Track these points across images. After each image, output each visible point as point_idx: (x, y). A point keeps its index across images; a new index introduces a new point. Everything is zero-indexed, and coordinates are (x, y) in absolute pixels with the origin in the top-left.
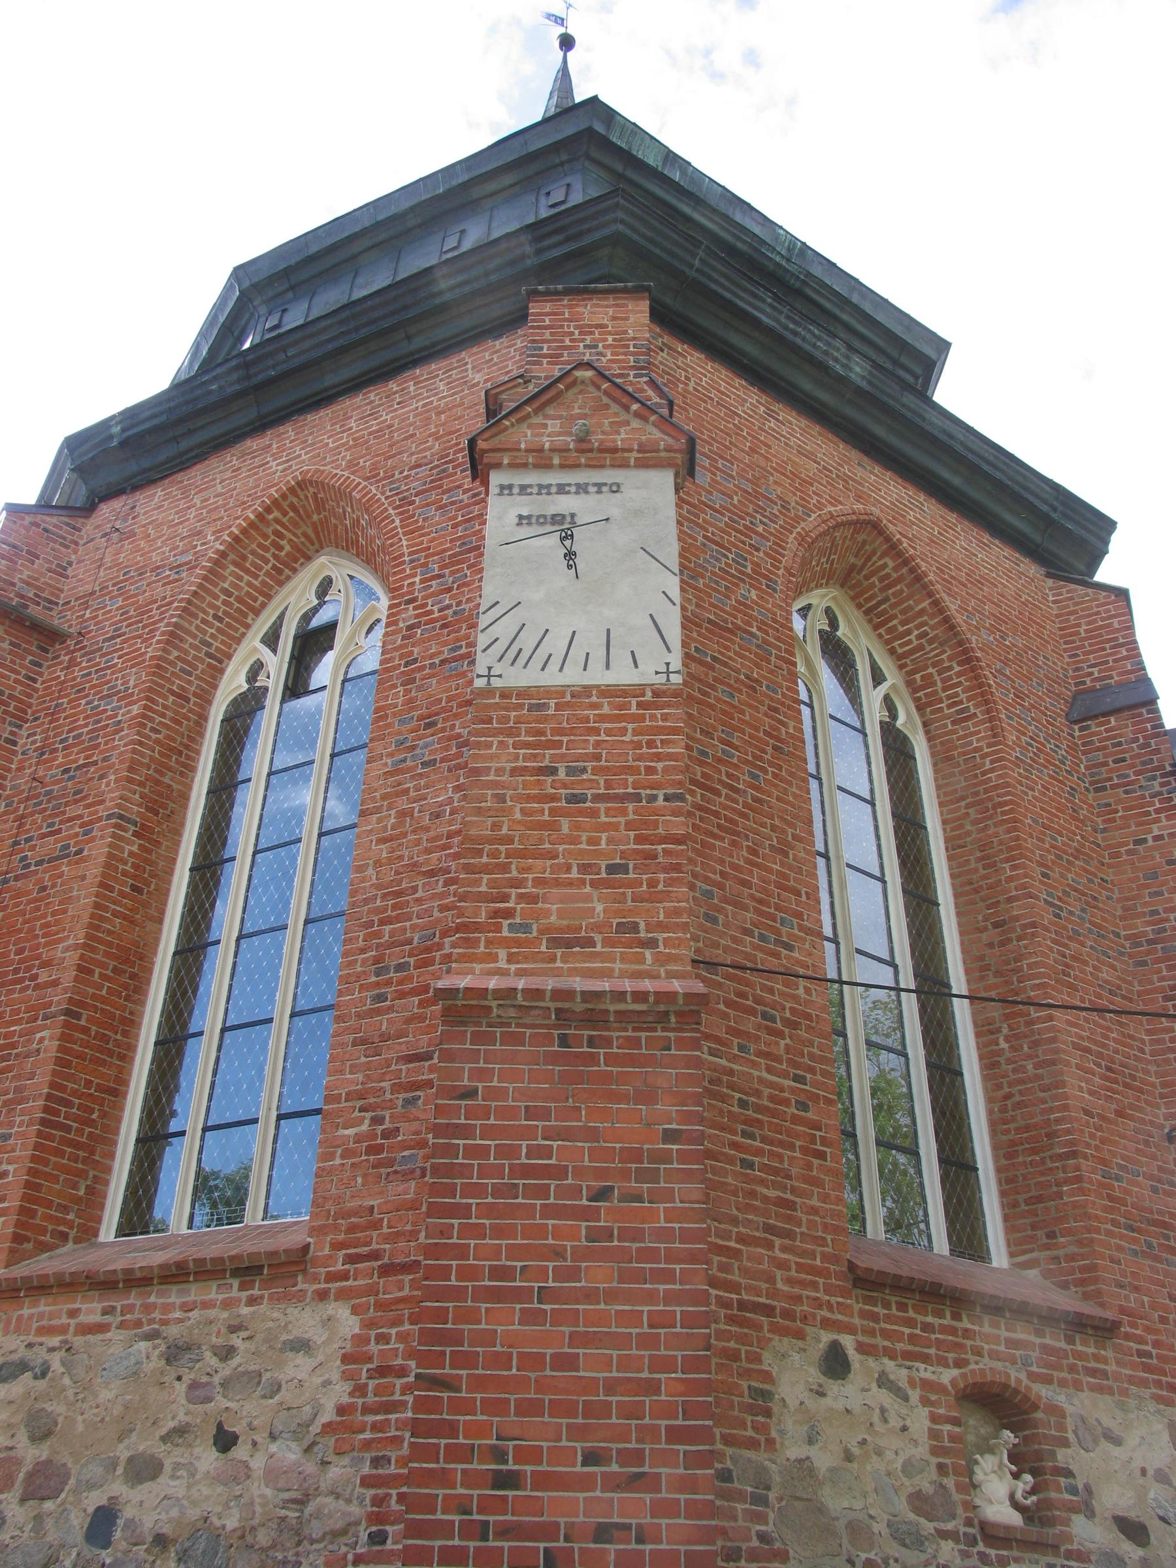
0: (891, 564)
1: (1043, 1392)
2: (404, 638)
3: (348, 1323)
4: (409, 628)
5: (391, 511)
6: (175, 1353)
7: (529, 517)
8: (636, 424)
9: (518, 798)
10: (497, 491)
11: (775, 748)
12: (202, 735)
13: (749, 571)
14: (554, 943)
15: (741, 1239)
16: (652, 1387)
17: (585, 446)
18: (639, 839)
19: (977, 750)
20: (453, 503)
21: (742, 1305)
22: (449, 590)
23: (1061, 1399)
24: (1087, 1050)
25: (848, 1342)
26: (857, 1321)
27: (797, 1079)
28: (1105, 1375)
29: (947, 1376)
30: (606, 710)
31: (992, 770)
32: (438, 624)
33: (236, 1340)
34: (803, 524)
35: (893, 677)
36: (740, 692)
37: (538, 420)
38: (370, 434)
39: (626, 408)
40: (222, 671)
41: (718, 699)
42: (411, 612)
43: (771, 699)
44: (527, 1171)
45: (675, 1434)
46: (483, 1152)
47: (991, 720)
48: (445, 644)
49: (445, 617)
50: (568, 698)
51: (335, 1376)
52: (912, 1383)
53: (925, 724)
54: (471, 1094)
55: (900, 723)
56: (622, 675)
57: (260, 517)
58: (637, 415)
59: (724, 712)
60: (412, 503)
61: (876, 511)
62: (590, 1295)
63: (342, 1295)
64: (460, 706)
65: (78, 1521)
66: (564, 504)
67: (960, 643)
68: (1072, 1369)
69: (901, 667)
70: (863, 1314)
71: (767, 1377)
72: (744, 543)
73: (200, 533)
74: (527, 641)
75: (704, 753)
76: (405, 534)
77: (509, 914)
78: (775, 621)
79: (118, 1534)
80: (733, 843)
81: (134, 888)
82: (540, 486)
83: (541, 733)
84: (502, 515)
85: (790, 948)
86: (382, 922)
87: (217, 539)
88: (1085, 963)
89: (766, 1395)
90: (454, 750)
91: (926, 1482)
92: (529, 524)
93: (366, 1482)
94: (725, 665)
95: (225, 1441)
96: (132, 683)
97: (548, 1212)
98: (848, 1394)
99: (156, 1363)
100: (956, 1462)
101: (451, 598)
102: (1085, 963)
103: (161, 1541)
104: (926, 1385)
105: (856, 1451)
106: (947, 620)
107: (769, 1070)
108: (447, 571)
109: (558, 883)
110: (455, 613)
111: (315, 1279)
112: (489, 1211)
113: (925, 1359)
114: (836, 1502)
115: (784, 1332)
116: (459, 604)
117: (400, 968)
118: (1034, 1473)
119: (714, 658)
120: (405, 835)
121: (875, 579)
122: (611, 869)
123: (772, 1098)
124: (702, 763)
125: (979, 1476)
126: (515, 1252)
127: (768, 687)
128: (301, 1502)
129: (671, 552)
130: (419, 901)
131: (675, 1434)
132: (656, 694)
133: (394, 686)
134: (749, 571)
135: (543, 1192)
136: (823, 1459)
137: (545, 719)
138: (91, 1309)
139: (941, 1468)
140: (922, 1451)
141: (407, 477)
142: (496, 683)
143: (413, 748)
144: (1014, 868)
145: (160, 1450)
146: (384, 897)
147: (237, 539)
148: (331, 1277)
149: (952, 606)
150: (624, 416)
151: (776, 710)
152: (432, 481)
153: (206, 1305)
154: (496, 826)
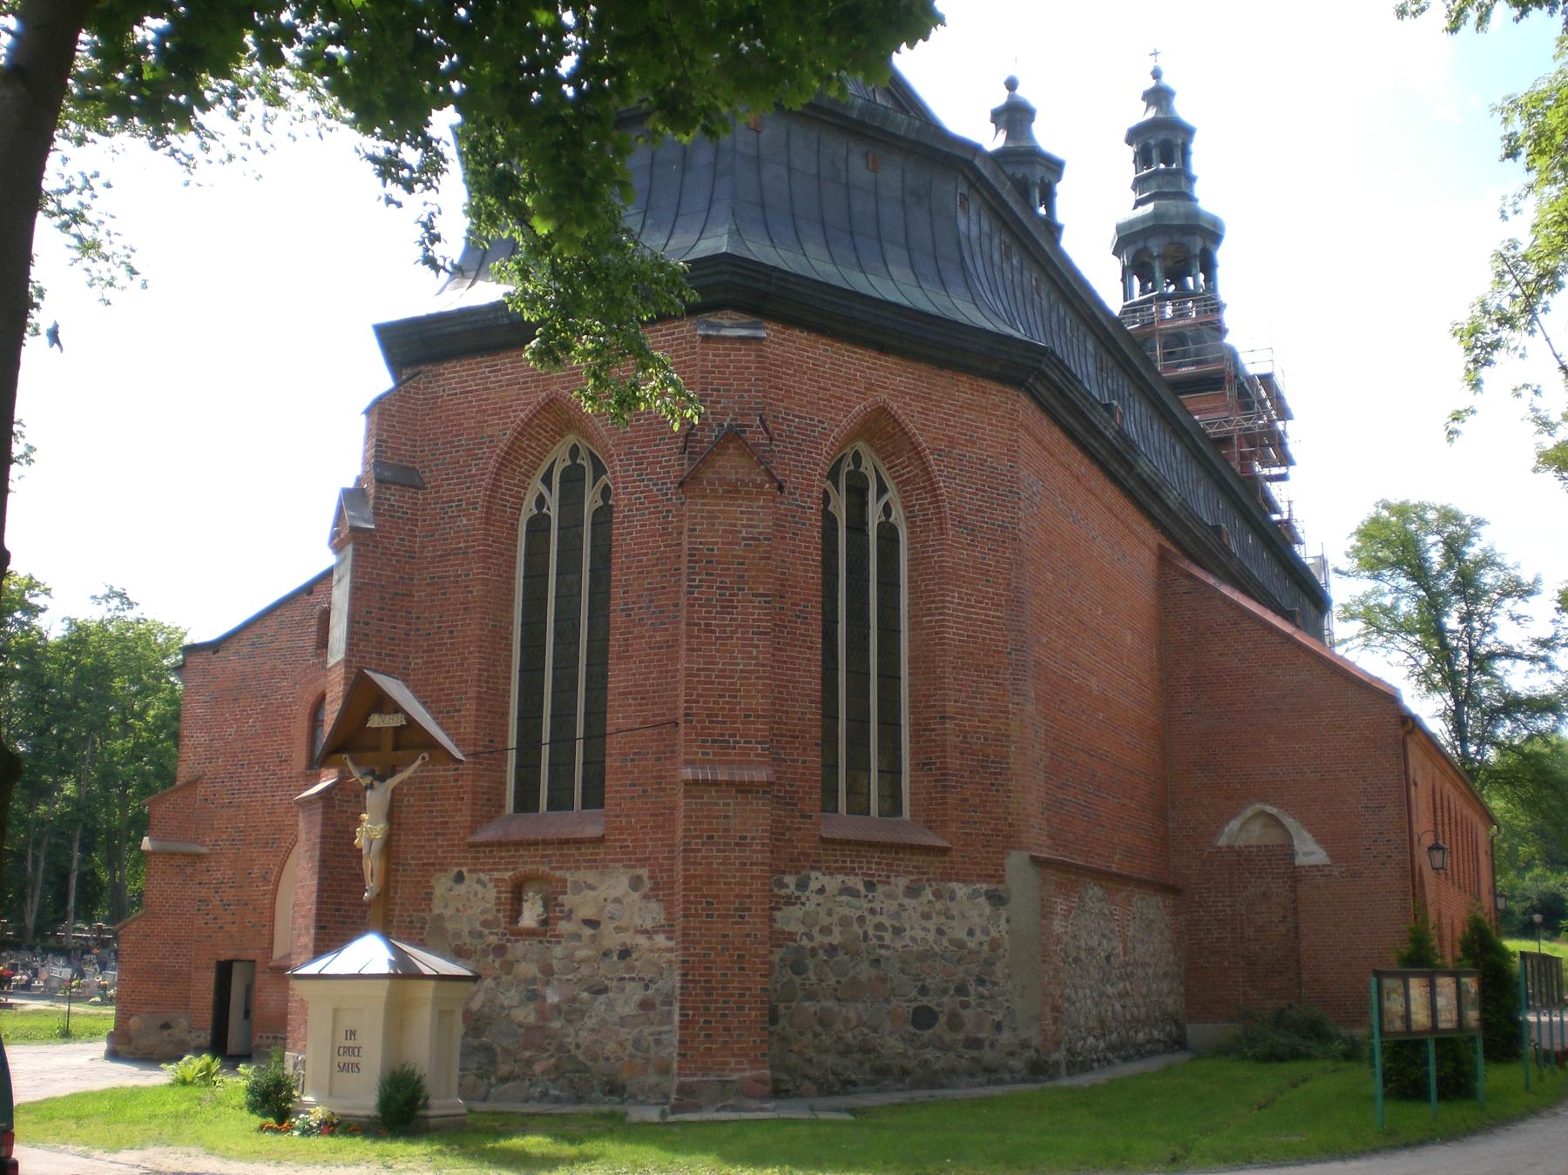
25: (464, 869)
29: (507, 875)
61: (555, 387)
91: (489, 917)
98: (462, 889)
114: (450, 926)
136: (448, 912)
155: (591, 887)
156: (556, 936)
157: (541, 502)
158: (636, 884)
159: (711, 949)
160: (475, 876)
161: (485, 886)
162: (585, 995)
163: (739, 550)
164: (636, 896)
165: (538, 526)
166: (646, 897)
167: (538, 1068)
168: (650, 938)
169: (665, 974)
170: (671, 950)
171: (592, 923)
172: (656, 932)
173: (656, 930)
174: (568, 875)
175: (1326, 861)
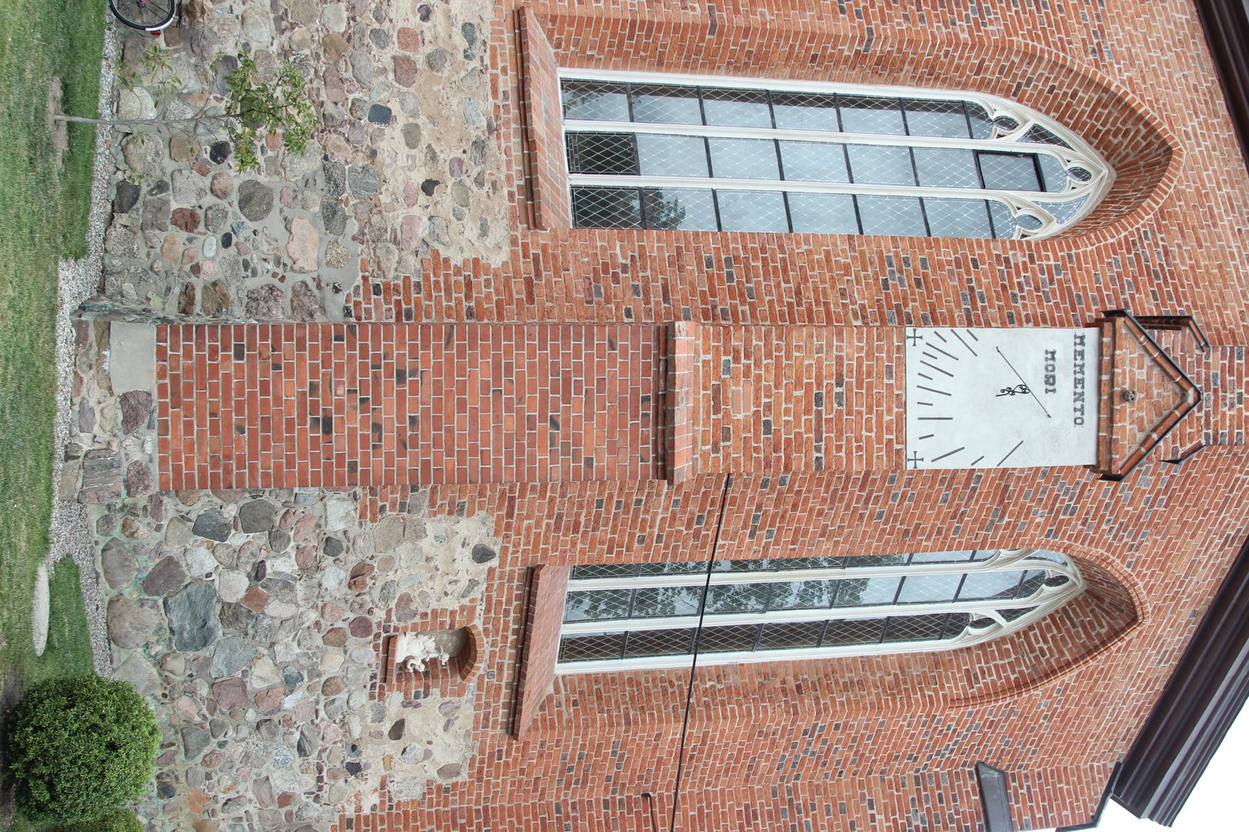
0: (1103, 631)
1: (472, 683)
2: (998, 256)
3: (497, 260)
4: (1007, 260)
5: (1124, 234)
6: (479, 145)
7: (1053, 359)
8: (1140, 436)
9: (819, 361)
10: (1079, 334)
11: (907, 532)
12: (950, 87)
13: (1061, 517)
14: (717, 390)
15: (552, 500)
16: (450, 453)
17: (1116, 399)
18: (788, 441)
19: (942, 686)
20: (1122, 286)
21: (512, 499)
22: (1037, 289)
23: (468, 695)
24: (704, 743)
25: (494, 563)
26: (508, 568)
27: (659, 537)
28: (486, 726)
29: (478, 623)
30: (886, 418)
31: (923, 696)
32: (1006, 283)
33: (488, 186)
34: (1118, 561)
35: (1009, 627)
36: (949, 507)
37: (1147, 361)
38: (1210, 208)
39: (1154, 430)
40: (1007, 96)
41: (939, 491)
42: (1021, 260)
43: (948, 530)
44: (567, 381)
45: (426, 464)
46: (577, 355)
47: (966, 699)
48: (988, 290)
49: (1012, 287)
50: (897, 392)
51: (466, 255)
52: (472, 600)
53: (968, 649)
54: (612, 346)
55: (968, 629)
56: (914, 428)
57: (1141, 118)
58: (1148, 437)
59: (929, 496)
60: (1129, 252)
61: (1148, 622)
62: (498, 418)
63: (514, 254)
64: (931, 304)
65: (380, 97)
66: (1065, 384)
67: (1033, 681)
68: (488, 705)
69: (1018, 634)
70: (512, 572)
71: (471, 513)
72: (1087, 513)
73: (1132, 65)
74: (943, 362)
75: (892, 480)
76: (1098, 249)
77: (737, 359)
78: (1019, 535)
79: (376, 126)
80: (824, 500)
81: (814, 57)
82: (1082, 366)
83: (869, 375)
84: (1061, 339)
85: (752, 535)
86: (764, 259)
87: (1123, 82)
88: (771, 749)
90: (894, 303)
92: (1047, 359)
93: (407, 279)
94: (971, 497)
95: (429, 187)
96: (989, 28)
97: (544, 395)
98: (464, 559)
99: (474, 134)
100: (428, 623)
101: (1029, 291)
102: (771, 749)
103: (374, 153)
104: (472, 610)
105: (432, 564)
106: (1054, 672)
107: (663, 519)
108: (1056, 286)
109: (757, 390)
110: (1014, 296)
111: (524, 236)
112: (543, 361)
113: (488, 610)
114: (403, 551)
115: (498, 523)
116: (1023, 298)
117: (730, 276)
118: (426, 674)
119: (974, 489)
120: (830, 271)
121: (1091, 617)
122: (767, 424)
123: (644, 520)
124: (884, 479)
125: (423, 638)
126: (520, 375)
127: (958, 528)
128: (395, 241)
129: (1018, 462)
130: (778, 285)
131: (426, 464)
132: (898, 451)
133: (955, 252)
134: (1061, 517)
135: (555, 391)
136: (426, 544)
137: (879, 377)
138: (507, 83)
140: (434, 605)
141: (1157, 245)
142: (909, 342)
143: (901, 272)
144: (842, 704)
145: (423, 146)
146: (783, 260)
147: (1120, 100)
148: (525, 246)
149: (1069, 677)
150: (1148, 427)
151: (939, 532)
152: (1148, 267)
153: (509, 163)
154: (799, 348)
156: (381, 695)
162: (297, 735)
164: (432, 773)
166: (430, 783)
167: (184, 703)
170: (359, 809)
171: (398, 730)
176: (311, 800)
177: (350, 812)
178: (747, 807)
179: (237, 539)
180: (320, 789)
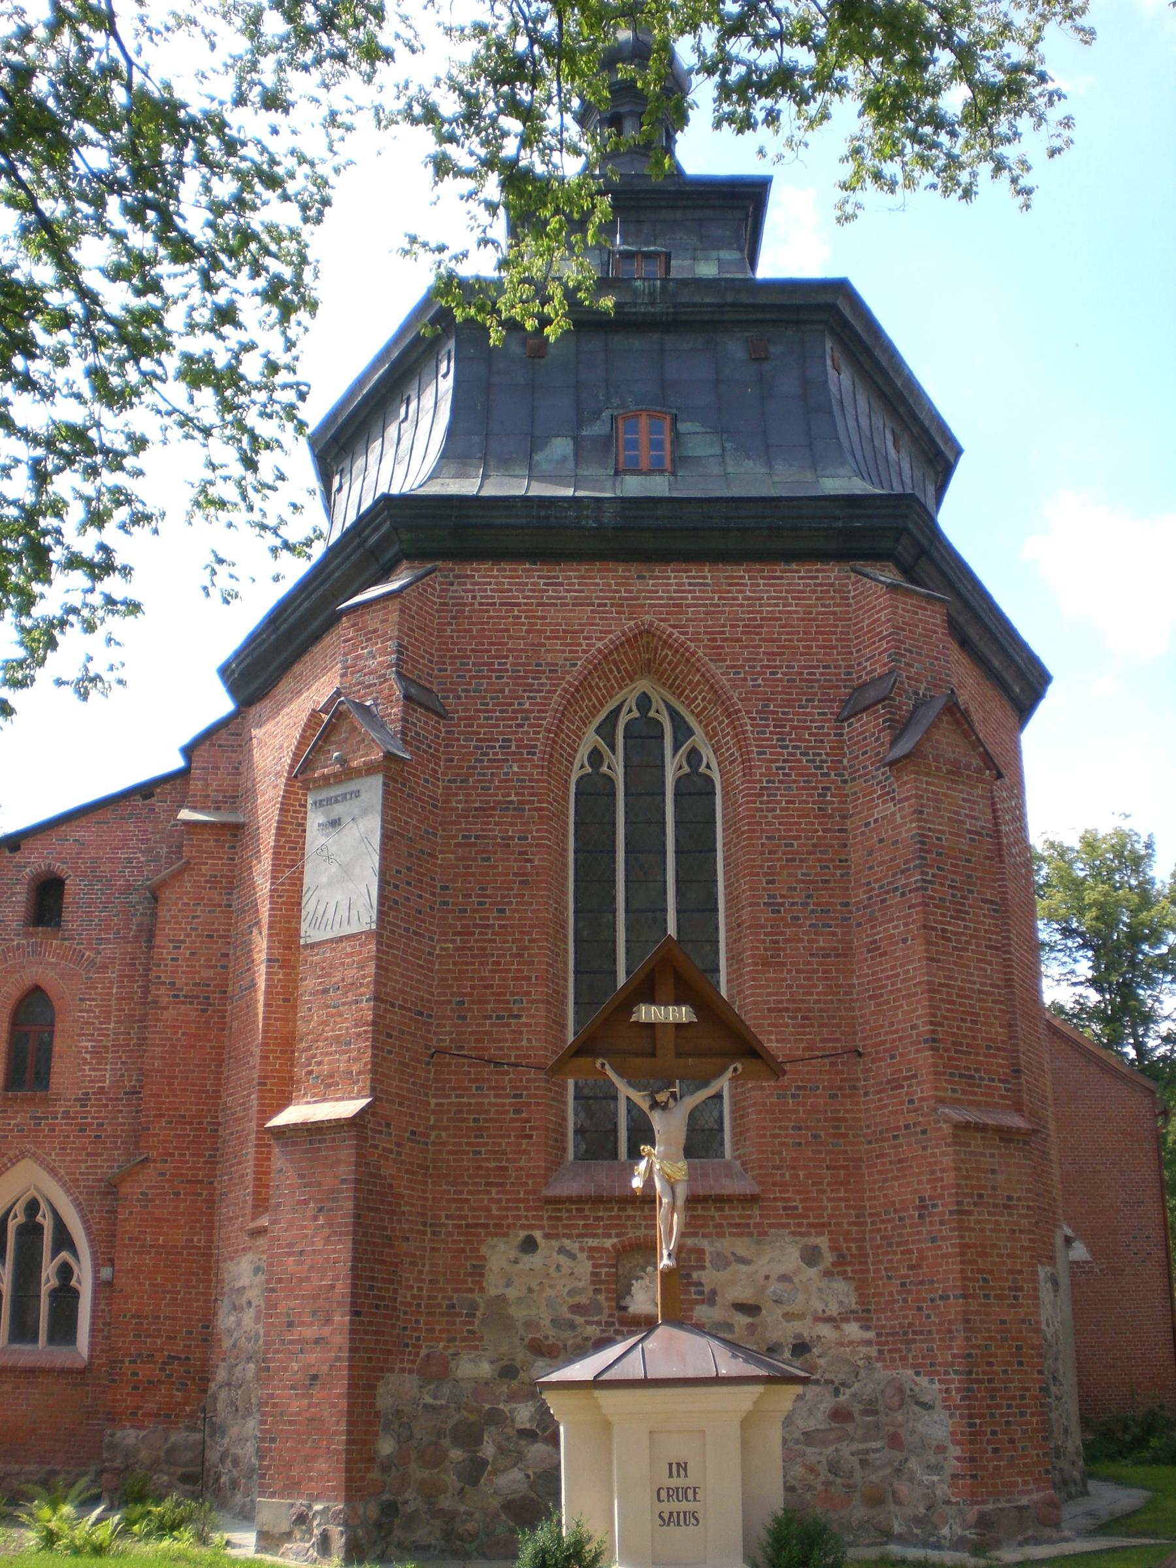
15: (469, 1192)
21: (468, 1226)
25: (537, 1234)
26: (545, 1223)
29: (608, 1243)
52: (582, 1249)
61: (647, 617)
71: (484, 1258)
80: (482, 964)
81: (285, 1000)
89: (483, 1267)
91: (583, 1300)
94: (485, 837)
98: (535, 1260)
105: (535, 1288)
107: (496, 1096)
113: (594, 1235)
114: (518, 1313)
115: (496, 1235)
123: (496, 1112)
136: (512, 1293)
139: (597, 1291)
155: (742, 1260)
157: (596, 757)
158: (811, 1256)
159: (991, 1338)
160: (555, 1244)
161: (572, 1256)
163: (964, 844)
164: (813, 1272)
165: (594, 792)
168: (837, 1328)
169: (863, 1373)
170: (868, 1343)
172: (847, 1320)
173: (845, 1317)
174: (705, 1244)
175: (1088, 1257)
176: (848, 1391)
177: (873, 1351)
178: (869, 951)
179: (488, 1450)
180: (832, 1382)
